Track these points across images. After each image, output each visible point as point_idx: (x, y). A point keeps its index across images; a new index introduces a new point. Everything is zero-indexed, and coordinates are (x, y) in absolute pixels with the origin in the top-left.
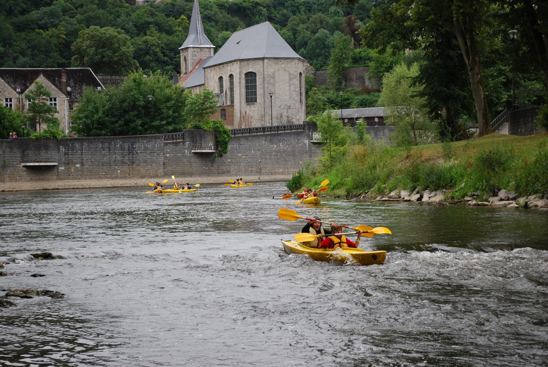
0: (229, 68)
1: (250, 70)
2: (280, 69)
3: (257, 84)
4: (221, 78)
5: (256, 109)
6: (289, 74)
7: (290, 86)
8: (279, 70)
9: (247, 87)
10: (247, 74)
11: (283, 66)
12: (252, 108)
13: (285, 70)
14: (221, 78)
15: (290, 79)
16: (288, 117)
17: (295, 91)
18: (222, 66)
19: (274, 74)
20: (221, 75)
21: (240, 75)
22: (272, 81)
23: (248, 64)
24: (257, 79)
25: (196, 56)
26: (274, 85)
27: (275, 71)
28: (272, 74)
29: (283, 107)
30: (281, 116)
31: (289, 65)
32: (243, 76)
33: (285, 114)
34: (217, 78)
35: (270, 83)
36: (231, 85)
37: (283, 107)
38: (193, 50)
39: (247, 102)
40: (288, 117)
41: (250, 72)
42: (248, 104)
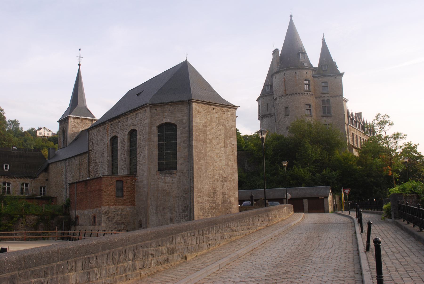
0: (129, 121)
1: (167, 120)
2: (214, 120)
3: (178, 141)
4: (114, 139)
5: (175, 180)
6: (225, 129)
7: (226, 147)
8: (211, 121)
9: (160, 147)
10: (161, 127)
11: (217, 116)
12: (169, 178)
13: (219, 123)
14: (114, 139)
15: (227, 137)
16: (224, 194)
17: (233, 155)
18: (117, 121)
19: (204, 126)
20: (114, 134)
21: (151, 128)
22: (202, 137)
23: (164, 112)
24: (178, 133)
25: (76, 127)
26: (205, 143)
27: (206, 123)
28: (201, 127)
29: (217, 177)
30: (215, 193)
31: (225, 116)
32: (155, 129)
33: (219, 189)
34: (107, 140)
35: (200, 141)
36: (130, 146)
37: (217, 177)
38: (73, 120)
39: (159, 169)
40: (224, 194)
41: (165, 124)
42: (161, 173)
